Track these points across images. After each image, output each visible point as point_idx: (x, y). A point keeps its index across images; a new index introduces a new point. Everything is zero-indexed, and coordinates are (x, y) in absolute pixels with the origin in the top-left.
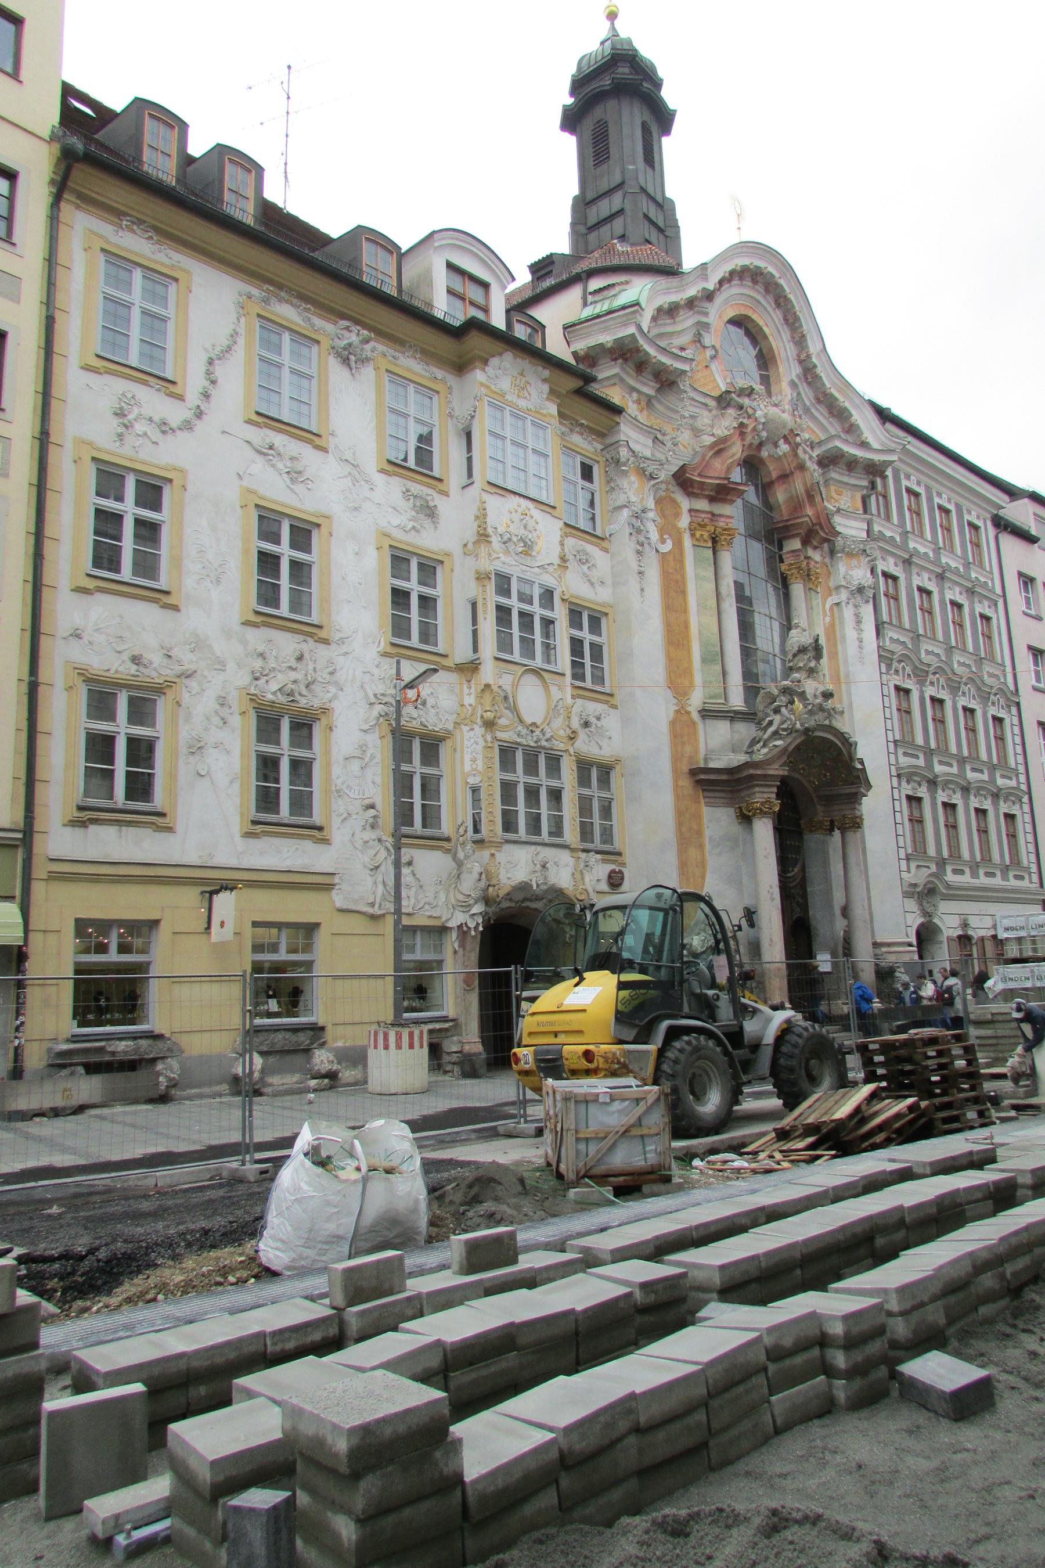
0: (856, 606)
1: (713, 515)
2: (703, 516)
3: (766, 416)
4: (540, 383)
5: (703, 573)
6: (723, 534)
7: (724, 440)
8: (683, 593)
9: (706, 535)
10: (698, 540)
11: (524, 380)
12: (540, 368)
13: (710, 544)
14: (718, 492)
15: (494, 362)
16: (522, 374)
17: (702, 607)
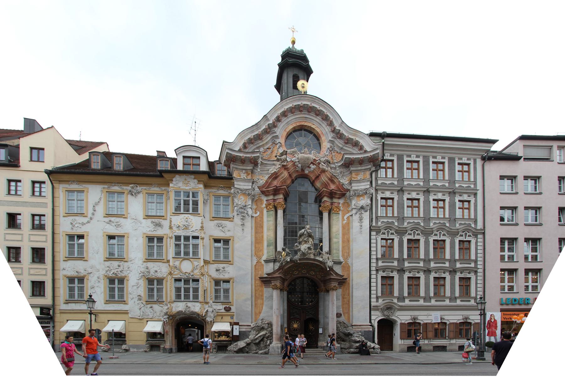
0: (360, 214)
1: (274, 199)
2: (270, 201)
3: (298, 158)
4: (193, 180)
5: (269, 219)
6: (278, 205)
7: (275, 173)
8: (262, 227)
9: (271, 207)
10: (269, 209)
11: (187, 181)
12: (190, 176)
13: (273, 209)
14: (274, 192)
15: (174, 179)
16: (186, 180)
17: (268, 230)
